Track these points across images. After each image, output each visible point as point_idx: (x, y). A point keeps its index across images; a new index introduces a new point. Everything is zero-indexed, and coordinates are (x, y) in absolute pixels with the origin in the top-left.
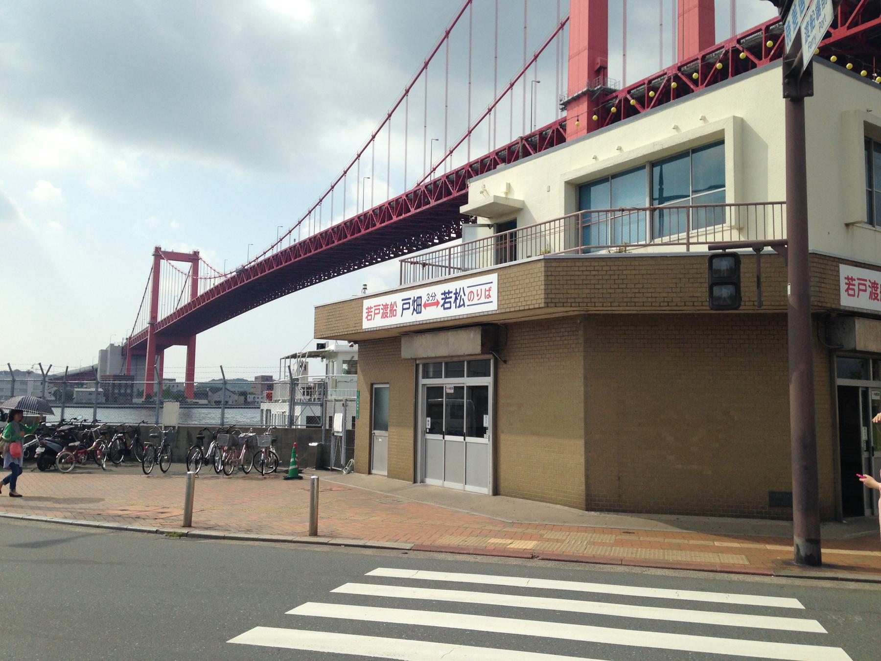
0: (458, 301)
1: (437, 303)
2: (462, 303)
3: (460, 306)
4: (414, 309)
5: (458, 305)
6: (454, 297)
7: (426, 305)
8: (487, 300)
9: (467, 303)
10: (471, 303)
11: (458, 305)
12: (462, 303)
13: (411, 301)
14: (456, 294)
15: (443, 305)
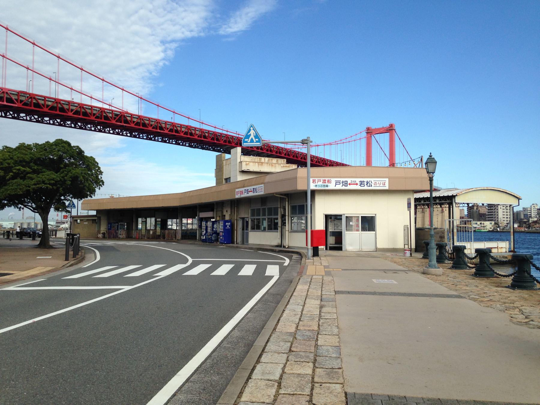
0: (368, 185)
1: (357, 184)
2: (370, 185)
3: (369, 186)
4: (343, 185)
5: (368, 185)
6: (366, 183)
7: (350, 184)
8: (383, 186)
9: (373, 185)
10: (375, 186)
11: (368, 185)
12: (370, 185)
13: (341, 182)
14: (367, 182)
15: (360, 185)
